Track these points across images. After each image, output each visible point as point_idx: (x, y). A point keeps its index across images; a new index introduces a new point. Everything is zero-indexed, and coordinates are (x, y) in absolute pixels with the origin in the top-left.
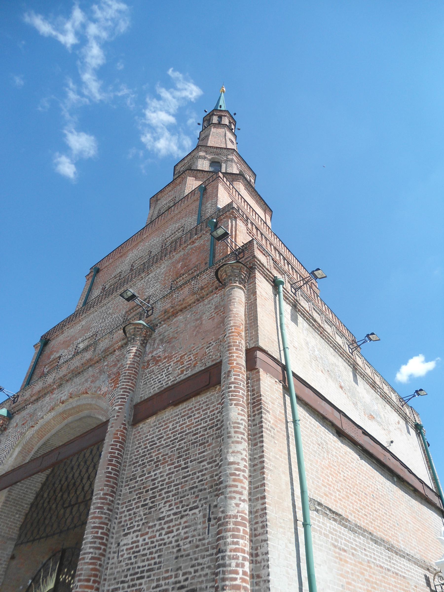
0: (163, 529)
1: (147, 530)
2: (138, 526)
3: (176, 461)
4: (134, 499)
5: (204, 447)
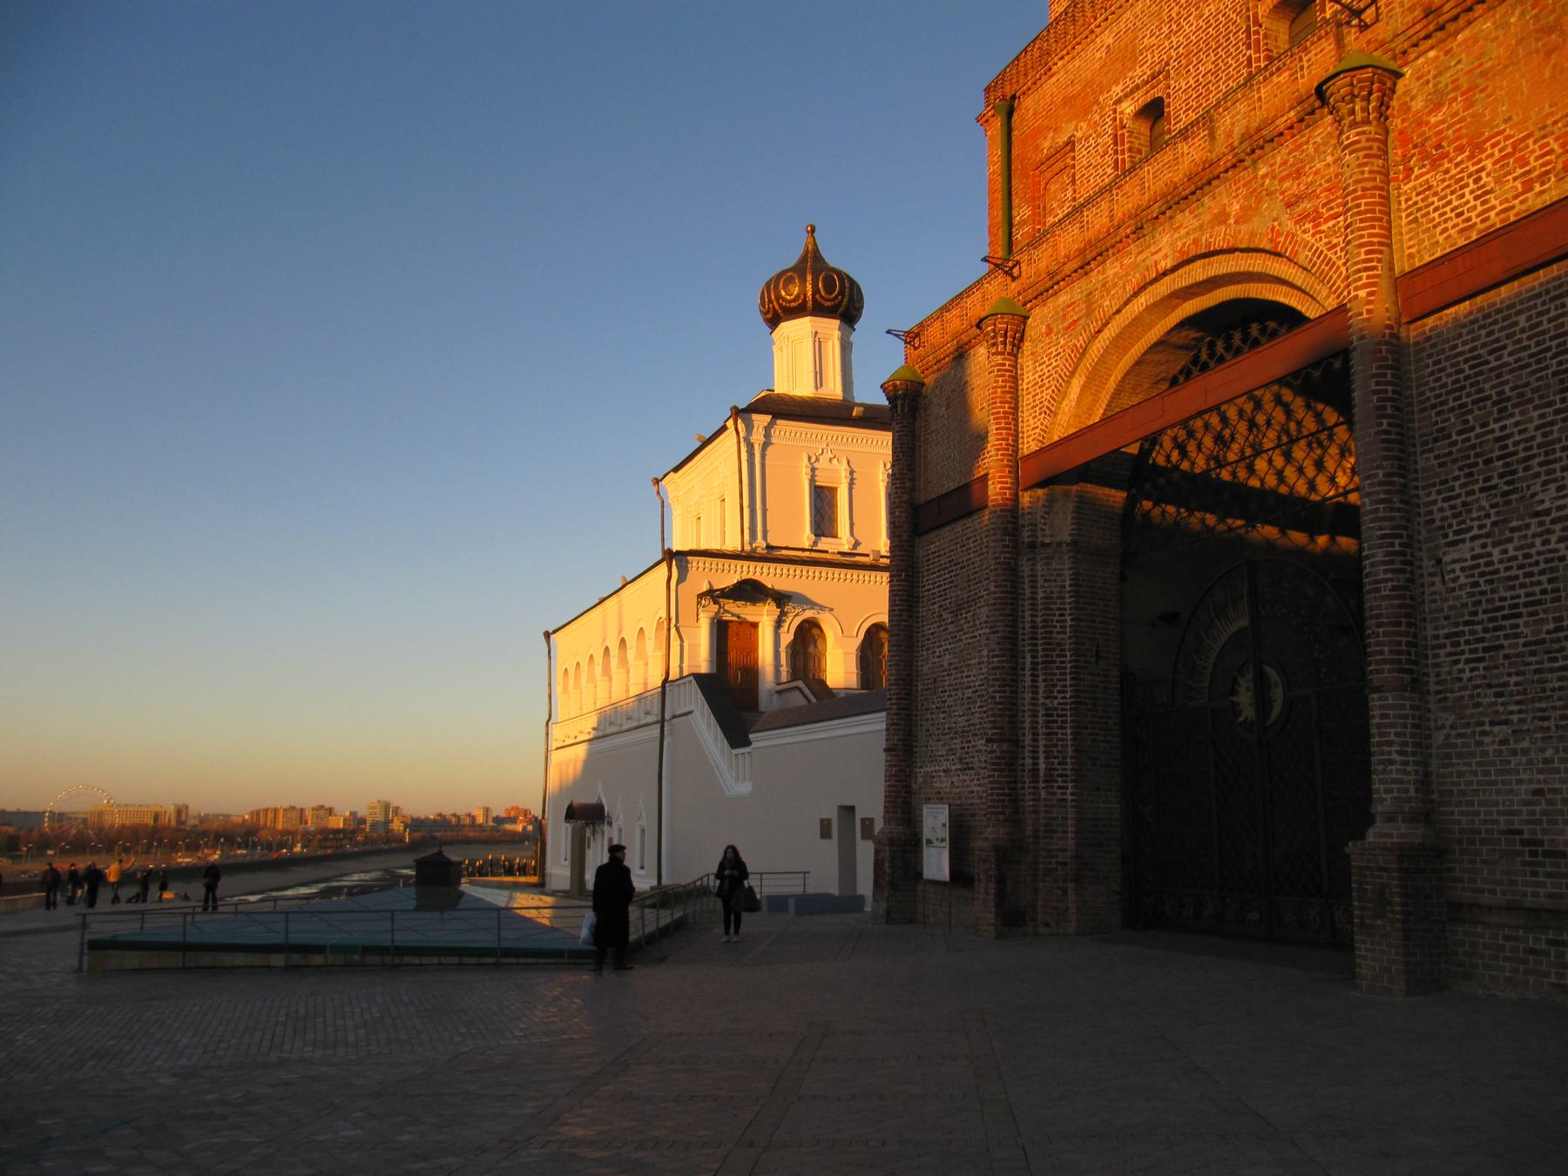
1: (1508, 534)
2: (1481, 527)
3: (1558, 398)
4: (1456, 478)
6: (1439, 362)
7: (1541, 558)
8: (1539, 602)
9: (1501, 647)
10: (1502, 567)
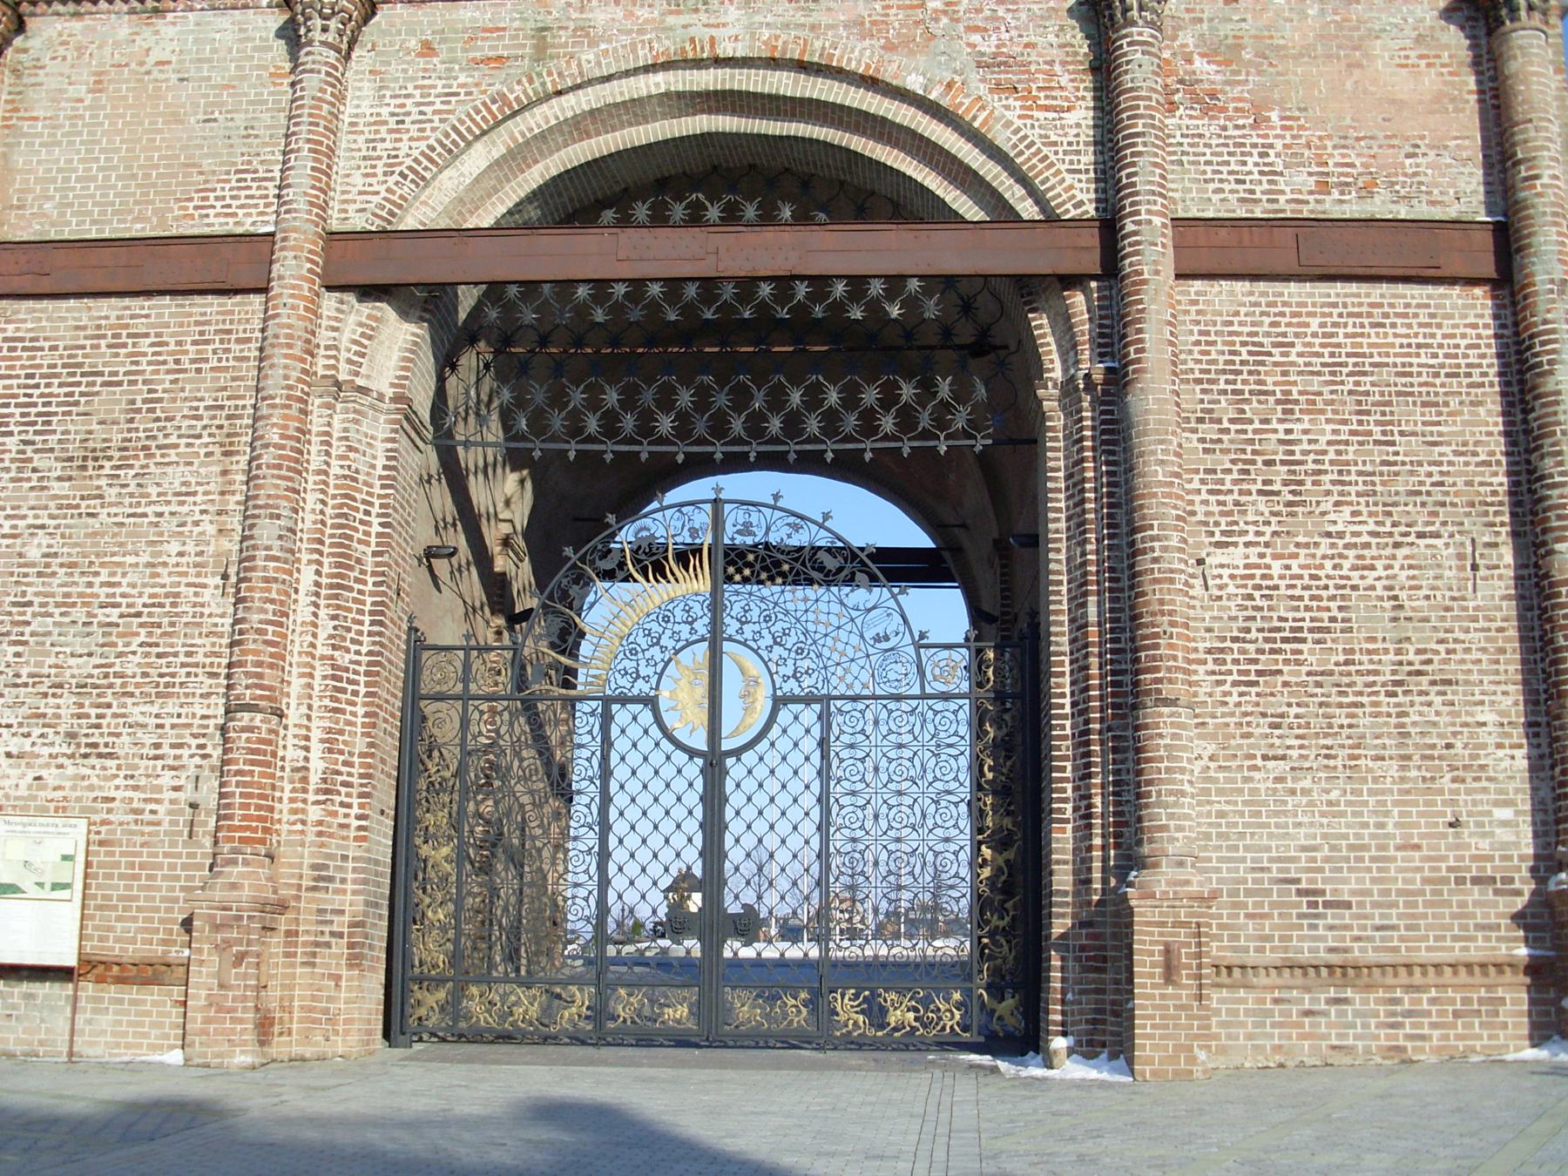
0: (1341, 556)
2: (1258, 533)
4: (1229, 471)
5: (1439, 414)
6: (1207, 333)
7: (1331, 583)
8: (1328, 630)
9: (1280, 672)
10: (1282, 583)
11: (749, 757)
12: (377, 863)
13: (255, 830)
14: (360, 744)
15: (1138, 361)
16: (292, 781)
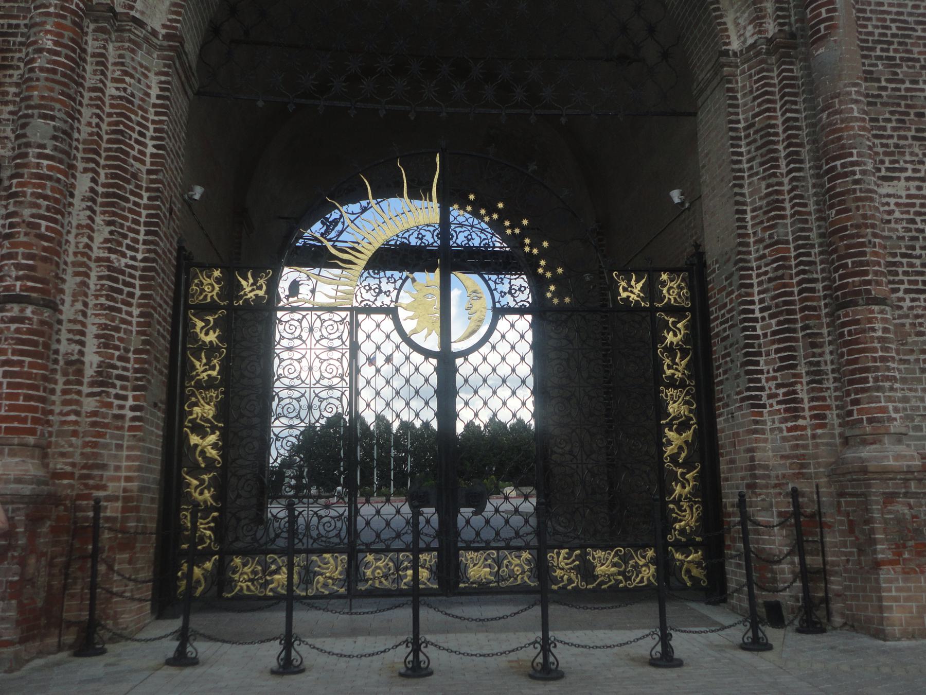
4: (889, 120)
6: (864, 11)
11: (475, 358)
12: (150, 451)
13: (24, 420)
14: (136, 342)
15: (831, 19)
16: (65, 374)
